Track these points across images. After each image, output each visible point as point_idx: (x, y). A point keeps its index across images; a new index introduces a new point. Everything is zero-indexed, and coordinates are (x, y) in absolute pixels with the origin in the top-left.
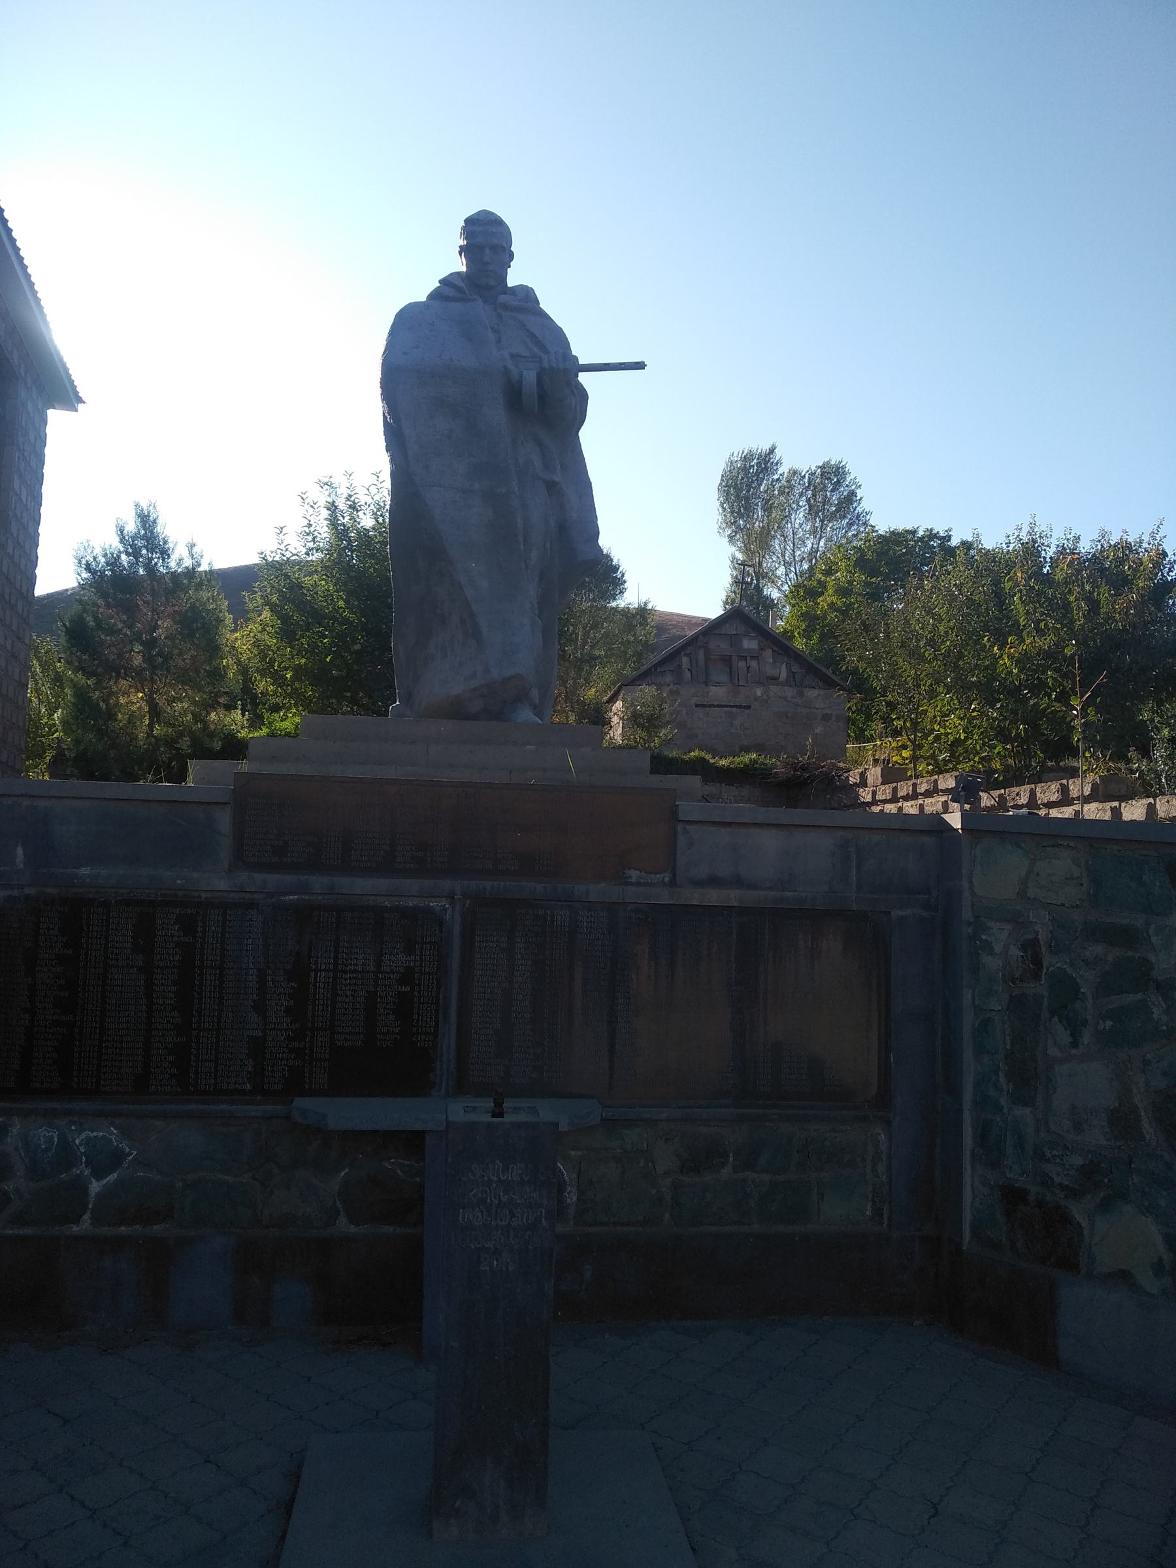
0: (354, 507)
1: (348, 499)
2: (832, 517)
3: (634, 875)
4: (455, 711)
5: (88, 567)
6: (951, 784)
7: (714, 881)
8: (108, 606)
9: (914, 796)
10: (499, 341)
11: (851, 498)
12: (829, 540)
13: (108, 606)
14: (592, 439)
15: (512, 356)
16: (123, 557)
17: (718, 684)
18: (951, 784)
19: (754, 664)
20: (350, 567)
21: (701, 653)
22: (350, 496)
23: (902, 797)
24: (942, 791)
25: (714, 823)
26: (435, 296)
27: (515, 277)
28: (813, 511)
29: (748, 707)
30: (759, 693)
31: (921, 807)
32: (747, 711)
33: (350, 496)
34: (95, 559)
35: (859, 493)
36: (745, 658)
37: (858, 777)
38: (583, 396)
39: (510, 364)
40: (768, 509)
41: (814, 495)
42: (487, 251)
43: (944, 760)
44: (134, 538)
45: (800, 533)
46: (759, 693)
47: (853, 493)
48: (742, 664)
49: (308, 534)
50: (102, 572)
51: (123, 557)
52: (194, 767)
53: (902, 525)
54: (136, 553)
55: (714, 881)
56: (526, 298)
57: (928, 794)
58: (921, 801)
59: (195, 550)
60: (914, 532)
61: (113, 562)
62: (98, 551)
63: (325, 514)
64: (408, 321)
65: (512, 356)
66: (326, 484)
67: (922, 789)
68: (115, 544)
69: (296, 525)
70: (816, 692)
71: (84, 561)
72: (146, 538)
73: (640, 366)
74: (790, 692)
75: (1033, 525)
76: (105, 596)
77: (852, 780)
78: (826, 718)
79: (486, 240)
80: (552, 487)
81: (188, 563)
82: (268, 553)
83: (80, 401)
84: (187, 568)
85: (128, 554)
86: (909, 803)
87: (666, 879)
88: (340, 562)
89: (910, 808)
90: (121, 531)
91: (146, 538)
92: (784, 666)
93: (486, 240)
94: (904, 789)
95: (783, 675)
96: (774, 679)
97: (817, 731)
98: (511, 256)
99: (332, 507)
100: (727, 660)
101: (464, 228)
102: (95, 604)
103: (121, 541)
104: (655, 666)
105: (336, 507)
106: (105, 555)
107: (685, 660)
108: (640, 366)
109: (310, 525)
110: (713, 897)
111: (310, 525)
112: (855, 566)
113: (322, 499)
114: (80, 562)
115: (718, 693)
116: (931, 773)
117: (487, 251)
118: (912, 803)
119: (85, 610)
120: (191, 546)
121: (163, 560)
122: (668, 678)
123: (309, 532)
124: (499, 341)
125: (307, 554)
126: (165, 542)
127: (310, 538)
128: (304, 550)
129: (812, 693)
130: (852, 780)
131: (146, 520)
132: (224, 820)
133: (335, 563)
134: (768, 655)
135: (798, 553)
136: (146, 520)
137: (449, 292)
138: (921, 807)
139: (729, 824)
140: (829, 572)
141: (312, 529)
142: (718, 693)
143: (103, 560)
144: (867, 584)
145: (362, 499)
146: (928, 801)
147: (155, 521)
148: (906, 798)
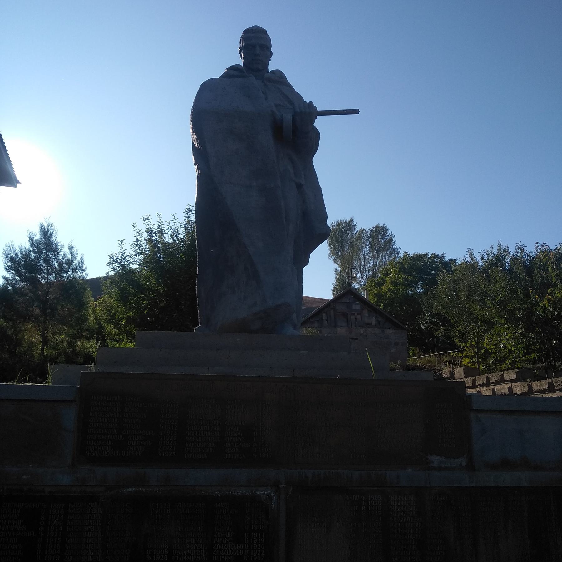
0: (161, 232)
1: (158, 228)
2: (382, 250)
3: (435, 460)
4: (242, 327)
5: (12, 260)
6: (513, 376)
7: (506, 464)
8: (22, 280)
9: (488, 384)
10: (266, 99)
11: (390, 242)
12: (381, 261)
13: (22, 280)
14: (320, 162)
15: (276, 105)
16: (32, 254)
17: (341, 327)
18: (513, 376)
19: (359, 317)
20: (158, 261)
21: (332, 312)
22: (160, 226)
23: (479, 385)
24: (507, 381)
25: (501, 412)
26: (224, 76)
27: (272, 67)
28: (372, 248)
29: (357, 339)
30: (362, 332)
31: (493, 391)
32: (356, 341)
33: (160, 226)
34: (15, 255)
35: (394, 239)
36: (354, 314)
37: (448, 374)
38: (317, 135)
39: (274, 109)
40: (351, 246)
41: (373, 241)
42: (258, 48)
43: (493, 363)
44: (39, 243)
45: (367, 257)
46: (362, 332)
47: (391, 240)
48: (353, 317)
49: (136, 245)
50: (19, 262)
51: (32, 254)
52: (52, 369)
53: (421, 252)
54: (40, 252)
55: (506, 464)
56: (279, 78)
57: (497, 383)
58: (492, 387)
59: (73, 250)
60: (426, 255)
61: (26, 256)
62: (18, 250)
63: (145, 235)
64: (208, 89)
65: (276, 105)
66: (146, 219)
67: (493, 380)
68: (28, 246)
69: (130, 239)
70: (390, 331)
71: (9, 256)
72: (46, 243)
73: (356, 112)
74: (377, 331)
75: (499, 245)
76: (18, 273)
77: (444, 376)
78: (396, 344)
79: (255, 44)
80: (299, 186)
81: (69, 257)
82: (114, 255)
83: (18, 182)
84: (68, 260)
85: (35, 252)
86: (485, 389)
87: (464, 464)
88: (154, 258)
89: (486, 392)
90: (31, 239)
91: (46, 243)
92: (374, 318)
93: (255, 44)
94: (480, 380)
95: (374, 323)
96: (369, 325)
97: (393, 351)
98: (271, 54)
99: (149, 231)
100: (345, 315)
101: (242, 37)
102: (15, 279)
103: (31, 246)
104: (309, 319)
105: (152, 231)
106: (22, 253)
107: (324, 315)
108: (356, 112)
109: (137, 240)
110: (507, 479)
111: (137, 240)
112: (399, 272)
113: (143, 227)
114: (7, 257)
115: (342, 332)
116: (485, 372)
117: (258, 48)
118: (487, 388)
119: (8, 284)
120: (71, 248)
121: (55, 255)
122: (316, 324)
123: (137, 244)
124: (266, 99)
125: (136, 255)
126: (56, 245)
127: (138, 248)
128: (134, 253)
129: (389, 332)
130: (444, 376)
131: (46, 233)
132: (70, 417)
133: (151, 260)
134: (366, 313)
135: (366, 267)
136: (46, 233)
137: (235, 73)
138: (493, 391)
139: (512, 412)
140: (386, 274)
141: (139, 243)
142: (342, 332)
143: (20, 255)
144: (406, 279)
145: (165, 227)
146: (497, 387)
147: (51, 235)
148: (482, 385)
